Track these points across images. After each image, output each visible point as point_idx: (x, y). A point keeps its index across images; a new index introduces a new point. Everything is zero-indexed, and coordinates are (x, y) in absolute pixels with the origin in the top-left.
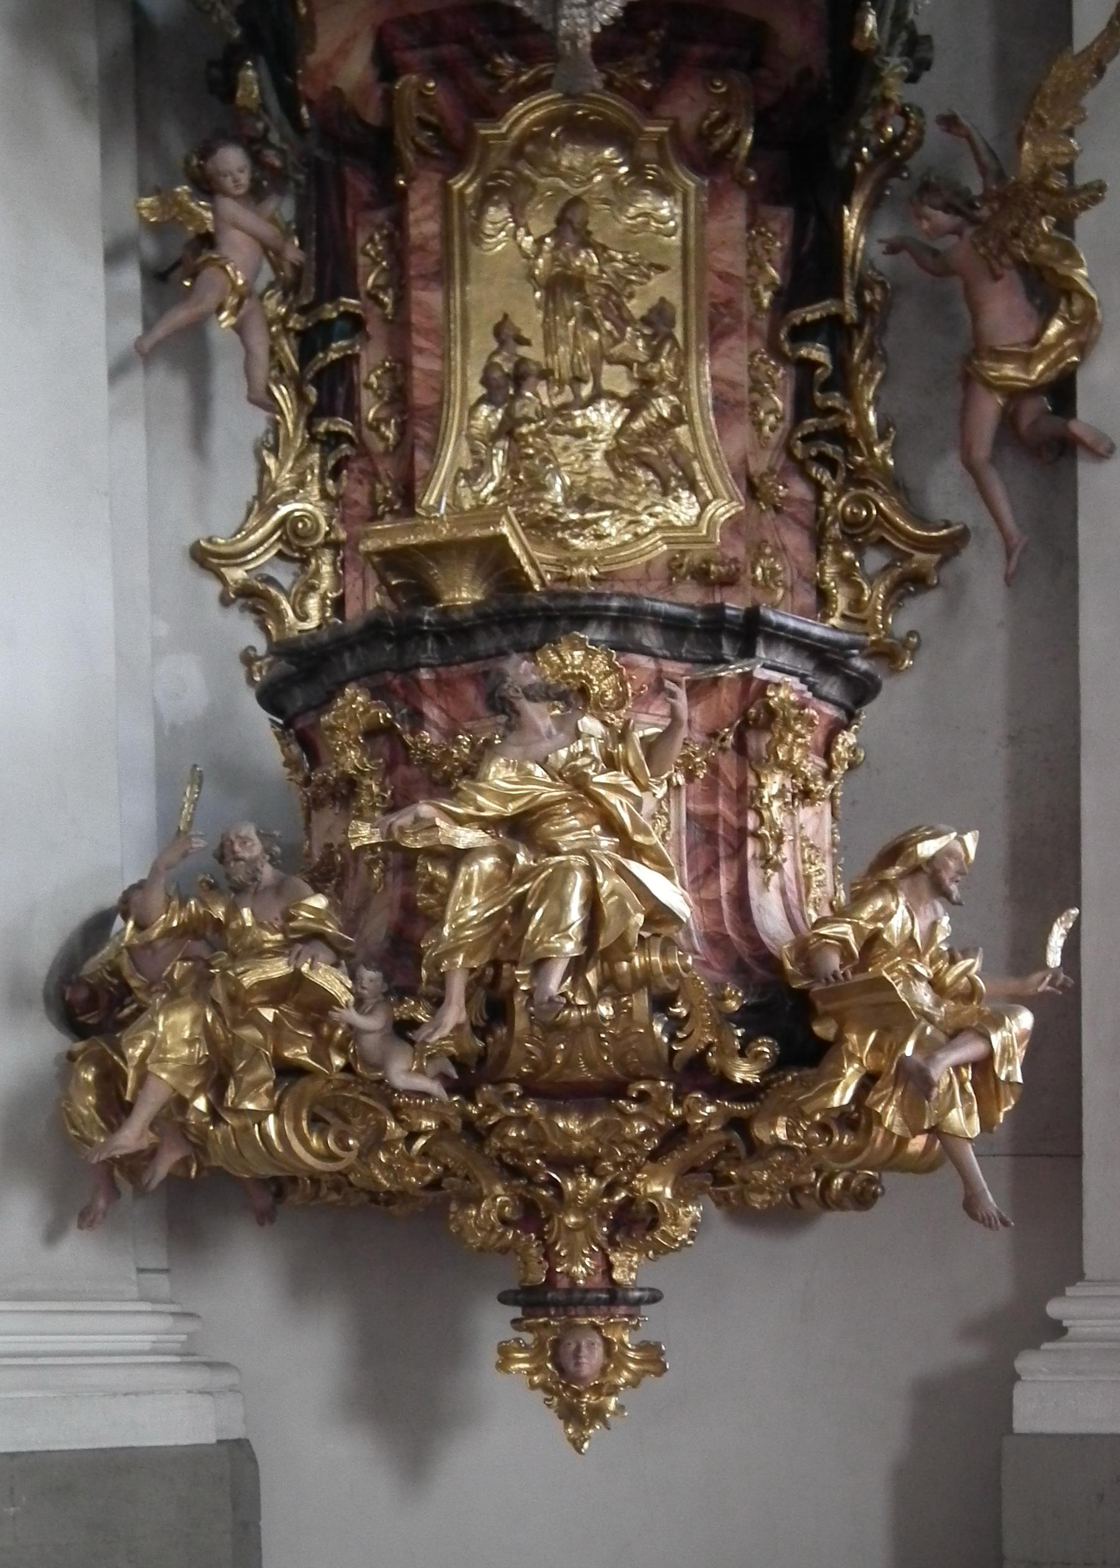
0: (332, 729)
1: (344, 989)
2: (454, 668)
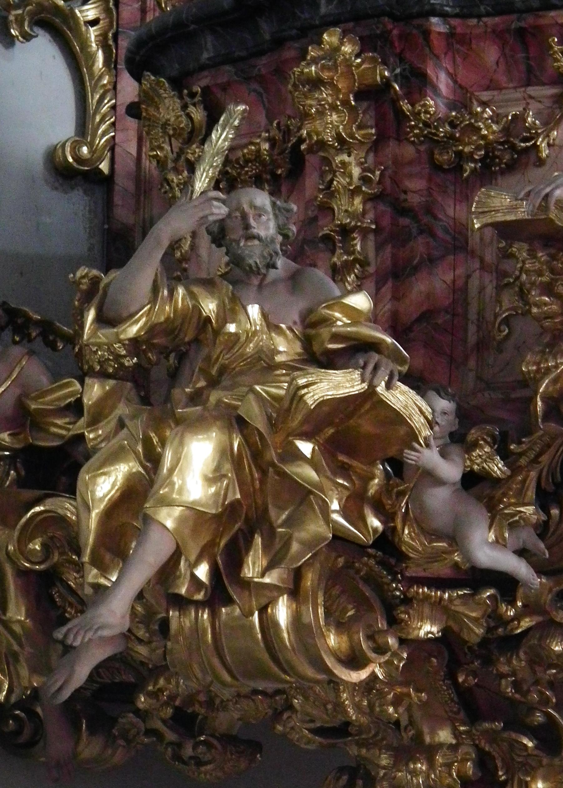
0: (316, 83)
1: (422, 420)
2: (474, 21)
